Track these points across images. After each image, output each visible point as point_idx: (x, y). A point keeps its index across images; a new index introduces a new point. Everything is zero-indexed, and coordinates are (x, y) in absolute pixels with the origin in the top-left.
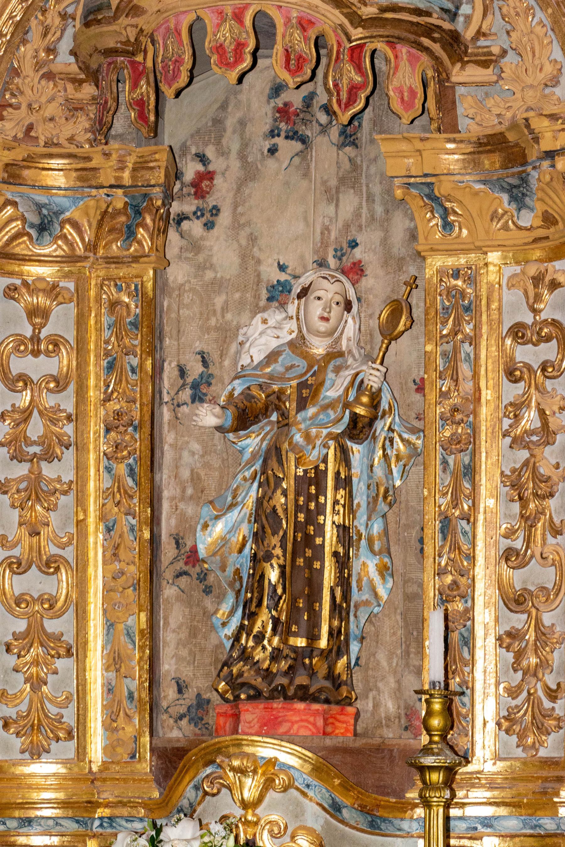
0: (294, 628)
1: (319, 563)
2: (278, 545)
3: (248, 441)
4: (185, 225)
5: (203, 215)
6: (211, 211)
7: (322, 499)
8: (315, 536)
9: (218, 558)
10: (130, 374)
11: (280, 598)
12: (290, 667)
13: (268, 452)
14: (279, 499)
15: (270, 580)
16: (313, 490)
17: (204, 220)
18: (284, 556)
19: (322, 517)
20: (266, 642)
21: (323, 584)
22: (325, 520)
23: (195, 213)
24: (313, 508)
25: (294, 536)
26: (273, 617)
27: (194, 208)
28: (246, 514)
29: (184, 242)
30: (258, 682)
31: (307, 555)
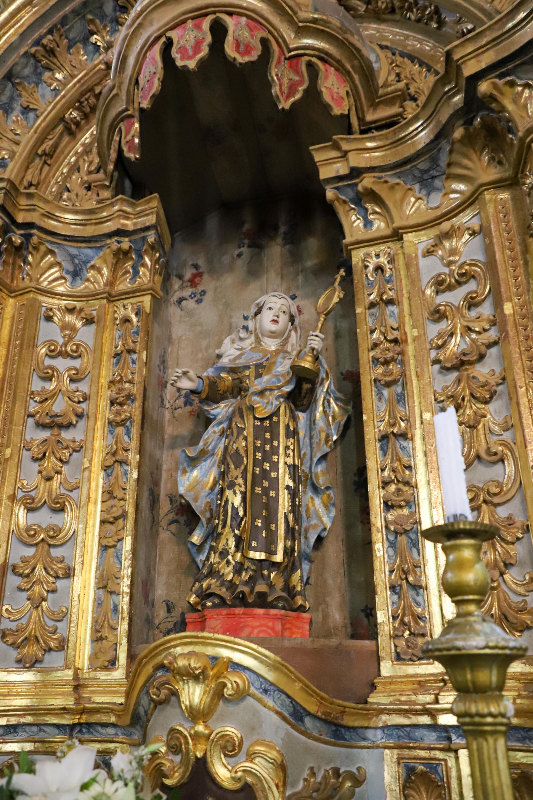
0: (254, 544)
1: (274, 492)
2: (240, 476)
3: (218, 410)
4: (184, 303)
5: (195, 296)
6: (200, 293)
7: (275, 443)
8: (271, 470)
9: (192, 493)
10: (131, 364)
11: (242, 519)
12: (251, 578)
13: (233, 412)
14: (241, 443)
15: (233, 504)
16: (268, 435)
17: (196, 299)
18: (245, 484)
19: (276, 457)
20: (230, 557)
21: (278, 509)
22: (278, 459)
23: (190, 296)
24: (268, 449)
25: (253, 469)
26: (235, 535)
27: (190, 293)
28: (216, 460)
29: (183, 313)
30: (223, 592)
31: (264, 485)
